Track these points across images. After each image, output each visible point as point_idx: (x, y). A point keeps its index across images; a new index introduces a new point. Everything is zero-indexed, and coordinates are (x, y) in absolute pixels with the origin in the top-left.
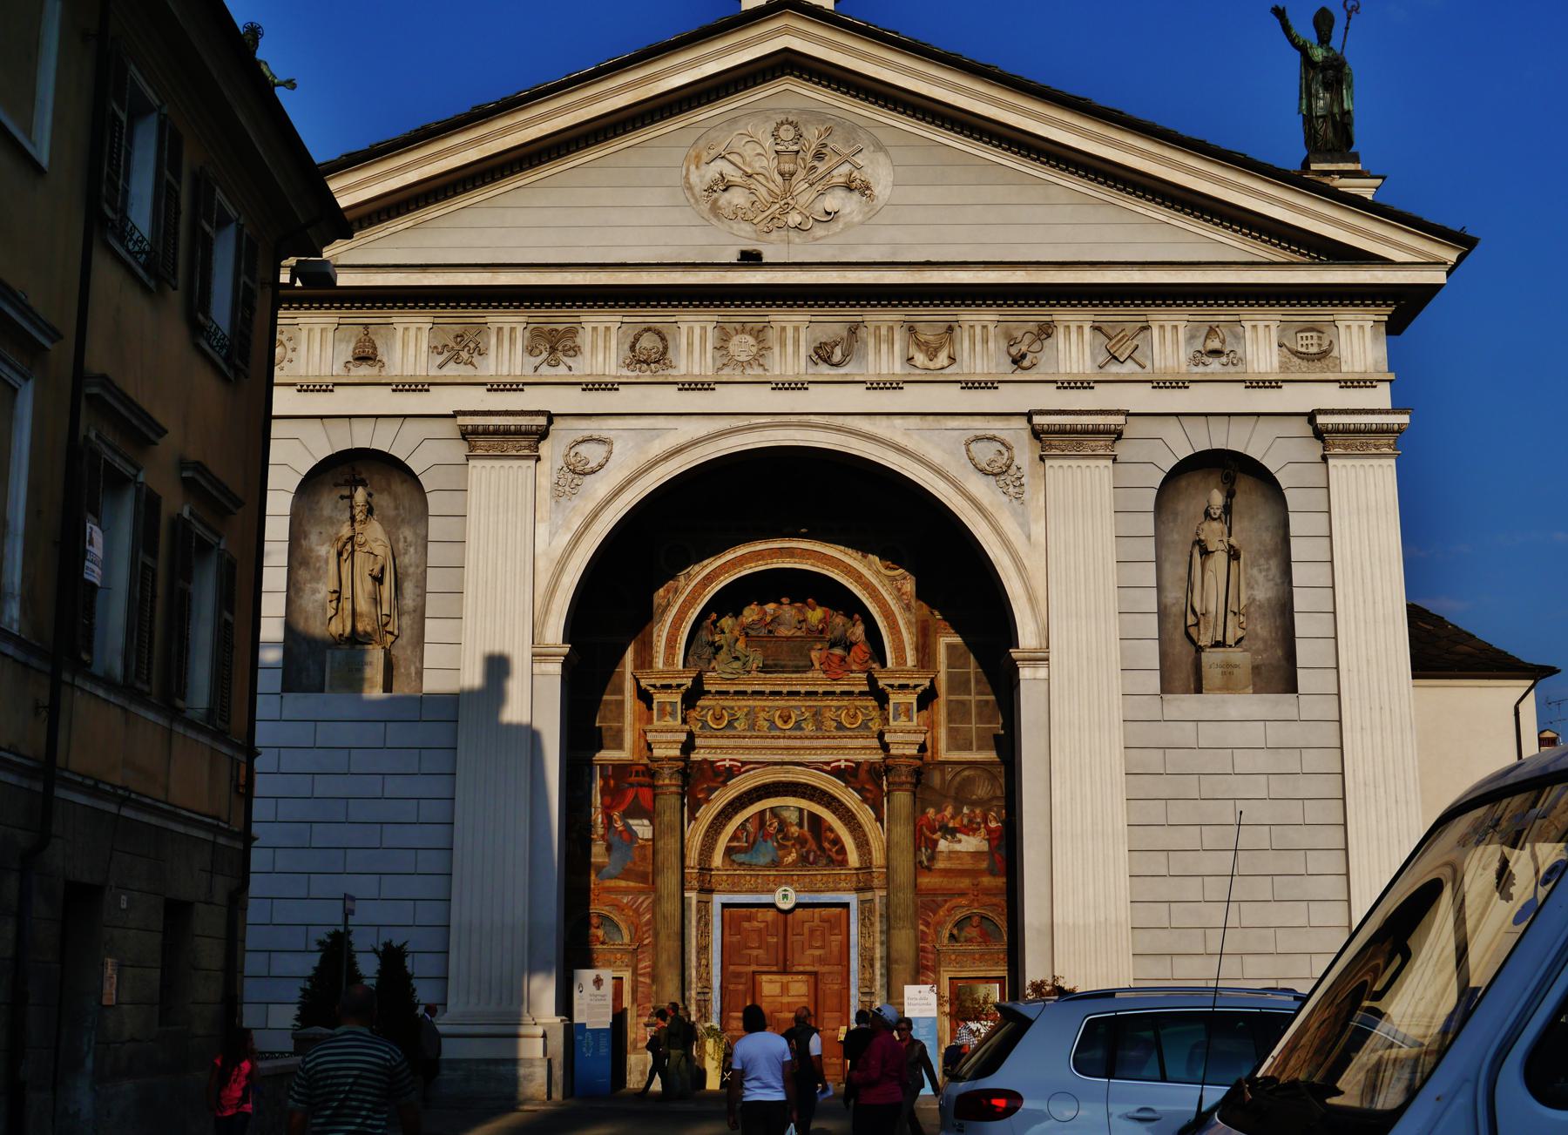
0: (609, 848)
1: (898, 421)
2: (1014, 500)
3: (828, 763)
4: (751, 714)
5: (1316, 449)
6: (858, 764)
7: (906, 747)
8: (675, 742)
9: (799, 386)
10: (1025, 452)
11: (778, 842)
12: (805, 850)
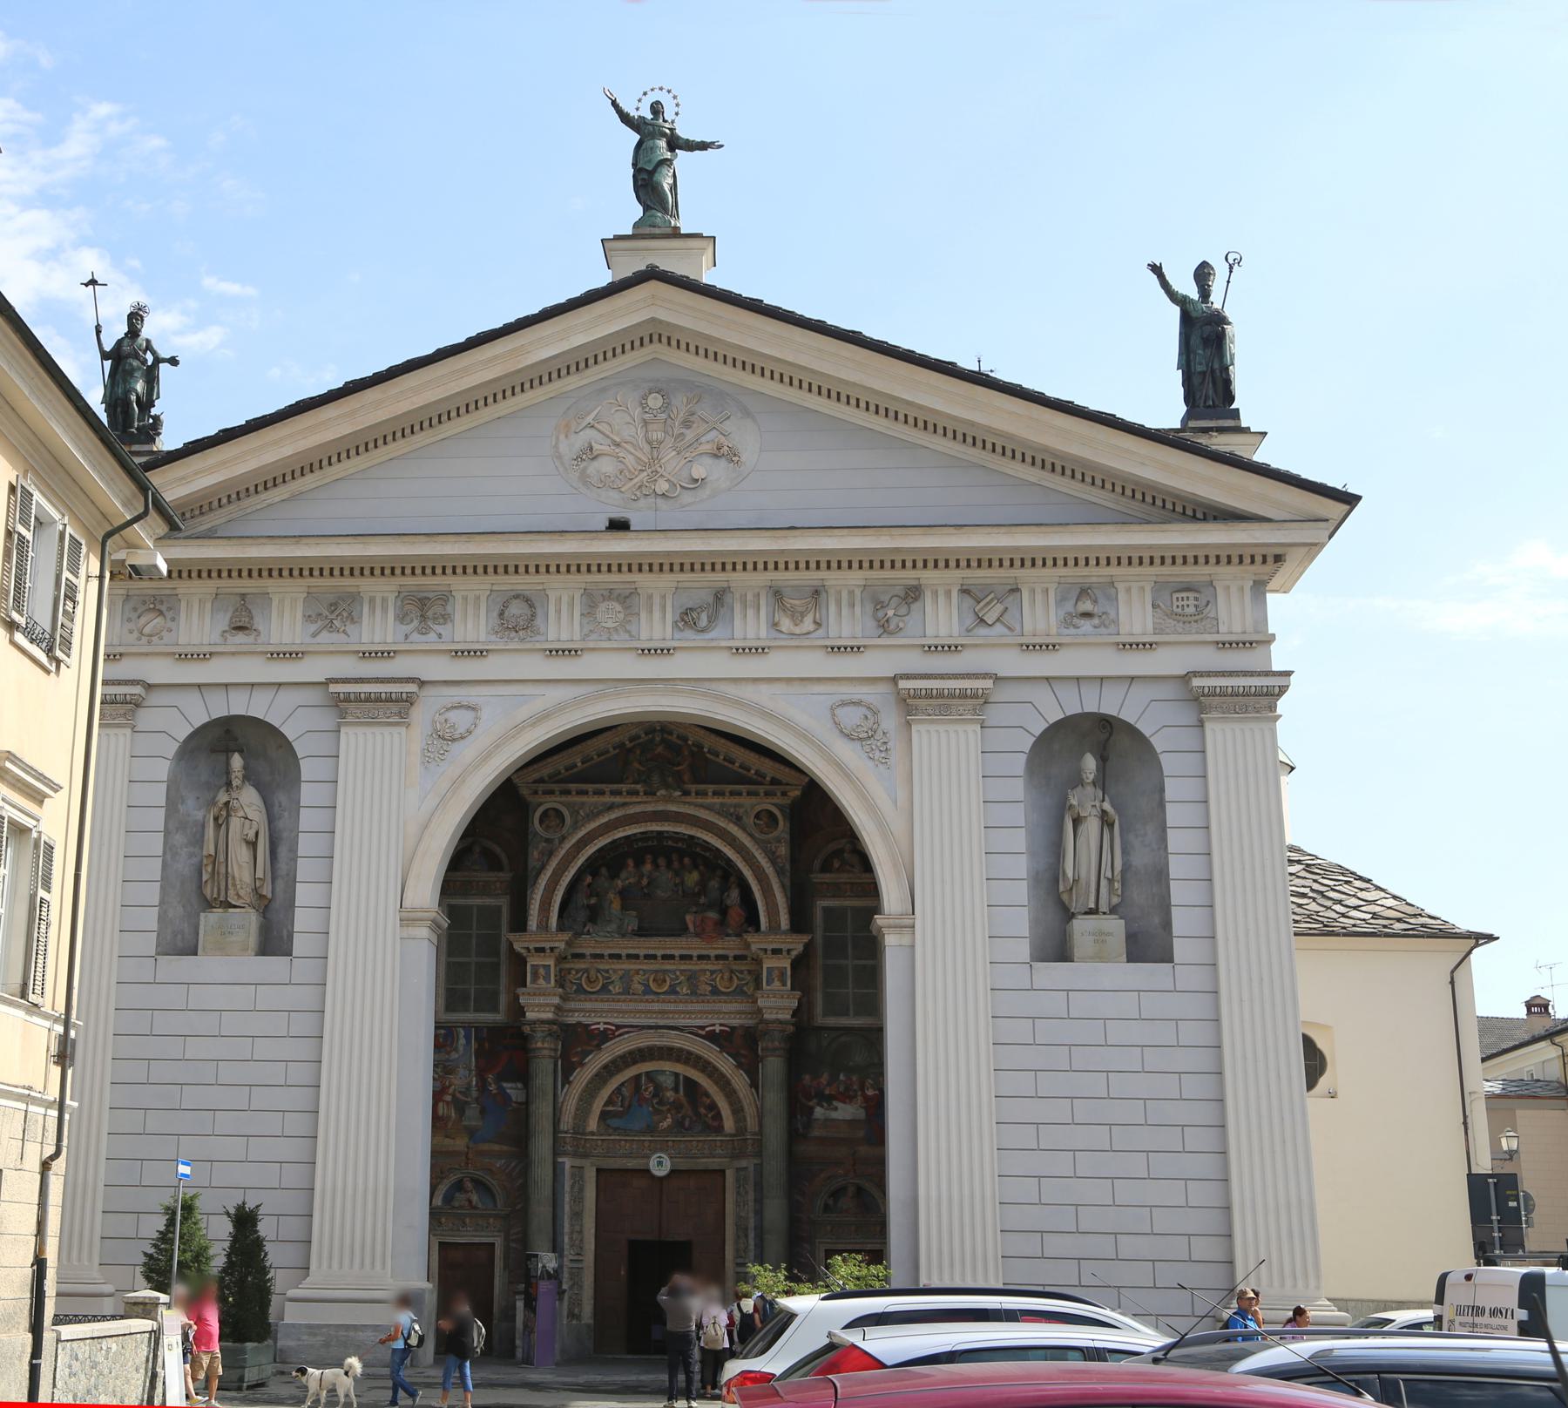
0: (483, 1112)
1: (764, 687)
2: (880, 765)
3: (702, 1028)
4: (626, 978)
5: (1187, 715)
6: (733, 1028)
7: (780, 1012)
8: (547, 1005)
9: (665, 652)
10: (890, 721)
11: (653, 1107)
12: (680, 1115)
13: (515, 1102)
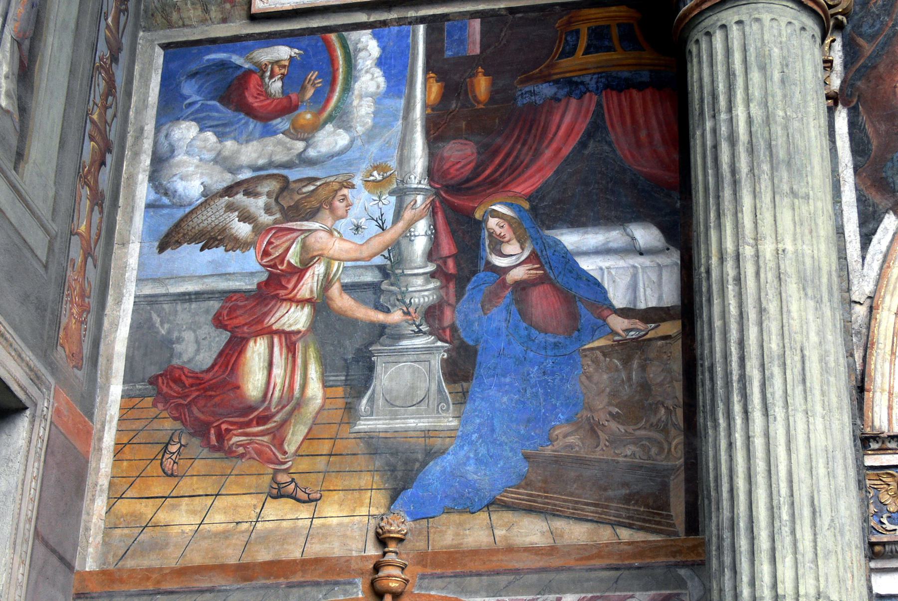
13: (625, 313)
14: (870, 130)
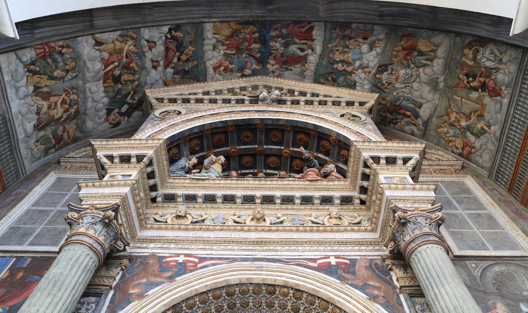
3: (314, 260)
6: (354, 262)
14: (117, 297)
